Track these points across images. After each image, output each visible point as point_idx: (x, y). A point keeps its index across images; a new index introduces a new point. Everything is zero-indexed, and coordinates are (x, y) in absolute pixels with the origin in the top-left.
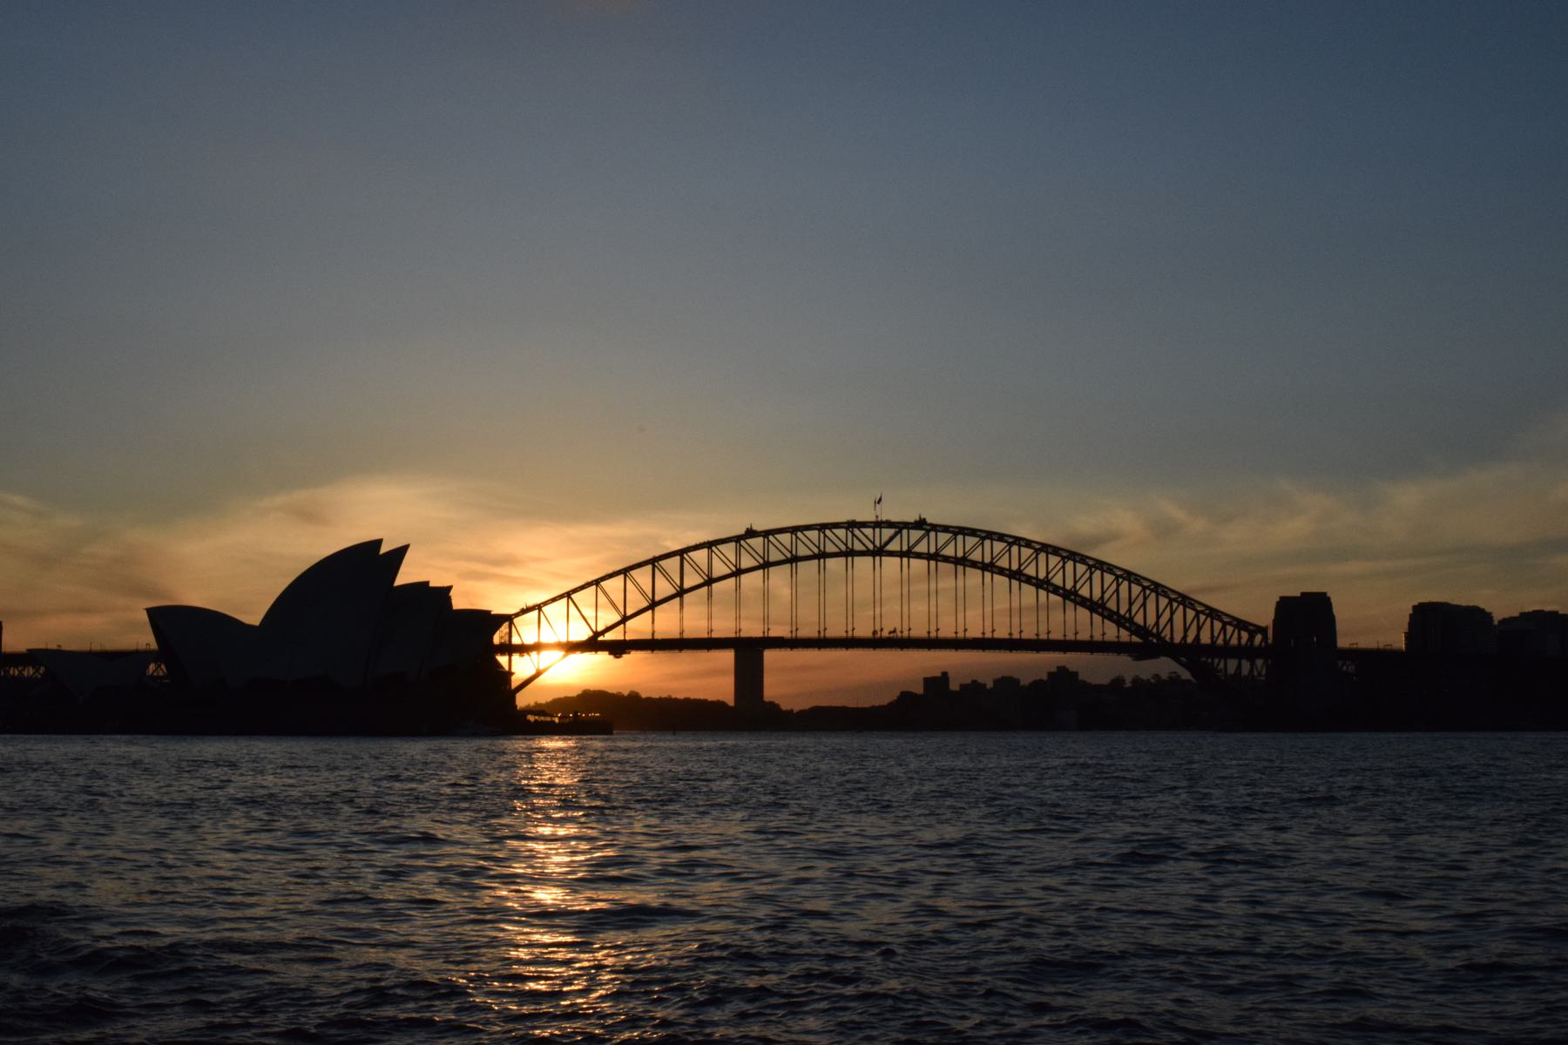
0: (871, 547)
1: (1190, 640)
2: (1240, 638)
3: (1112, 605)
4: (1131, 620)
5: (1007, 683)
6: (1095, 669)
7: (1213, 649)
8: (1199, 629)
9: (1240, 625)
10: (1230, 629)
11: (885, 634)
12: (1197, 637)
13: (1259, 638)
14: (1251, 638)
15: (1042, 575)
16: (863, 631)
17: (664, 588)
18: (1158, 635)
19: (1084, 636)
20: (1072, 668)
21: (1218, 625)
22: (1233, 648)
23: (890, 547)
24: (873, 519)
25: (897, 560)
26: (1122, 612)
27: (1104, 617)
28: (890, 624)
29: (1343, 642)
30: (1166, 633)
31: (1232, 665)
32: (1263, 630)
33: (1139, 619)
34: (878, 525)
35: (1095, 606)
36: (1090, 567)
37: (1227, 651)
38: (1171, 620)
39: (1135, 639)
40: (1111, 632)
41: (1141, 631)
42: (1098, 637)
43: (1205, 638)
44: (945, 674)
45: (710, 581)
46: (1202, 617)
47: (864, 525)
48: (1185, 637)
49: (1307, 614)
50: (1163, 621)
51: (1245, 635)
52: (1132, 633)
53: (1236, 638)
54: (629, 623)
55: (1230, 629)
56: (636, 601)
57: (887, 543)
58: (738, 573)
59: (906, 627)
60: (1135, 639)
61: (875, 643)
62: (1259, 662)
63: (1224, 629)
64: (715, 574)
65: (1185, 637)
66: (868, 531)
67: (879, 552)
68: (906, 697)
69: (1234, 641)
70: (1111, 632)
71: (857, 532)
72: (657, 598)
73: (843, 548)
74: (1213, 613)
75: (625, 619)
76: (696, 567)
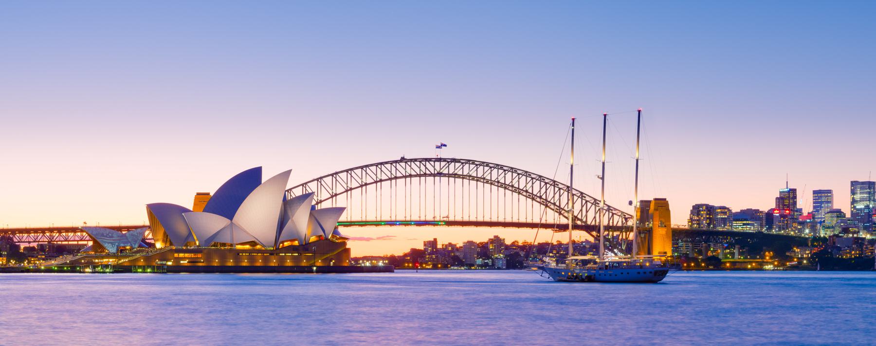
5: (470, 243)
6: (510, 236)
10: (616, 218)
20: (501, 237)
29: (672, 226)
34: (440, 160)
35: (546, 203)
36: (546, 183)
41: (575, 218)
42: (550, 221)
44: (435, 240)
53: (618, 221)
61: (419, 223)
69: (620, 224)
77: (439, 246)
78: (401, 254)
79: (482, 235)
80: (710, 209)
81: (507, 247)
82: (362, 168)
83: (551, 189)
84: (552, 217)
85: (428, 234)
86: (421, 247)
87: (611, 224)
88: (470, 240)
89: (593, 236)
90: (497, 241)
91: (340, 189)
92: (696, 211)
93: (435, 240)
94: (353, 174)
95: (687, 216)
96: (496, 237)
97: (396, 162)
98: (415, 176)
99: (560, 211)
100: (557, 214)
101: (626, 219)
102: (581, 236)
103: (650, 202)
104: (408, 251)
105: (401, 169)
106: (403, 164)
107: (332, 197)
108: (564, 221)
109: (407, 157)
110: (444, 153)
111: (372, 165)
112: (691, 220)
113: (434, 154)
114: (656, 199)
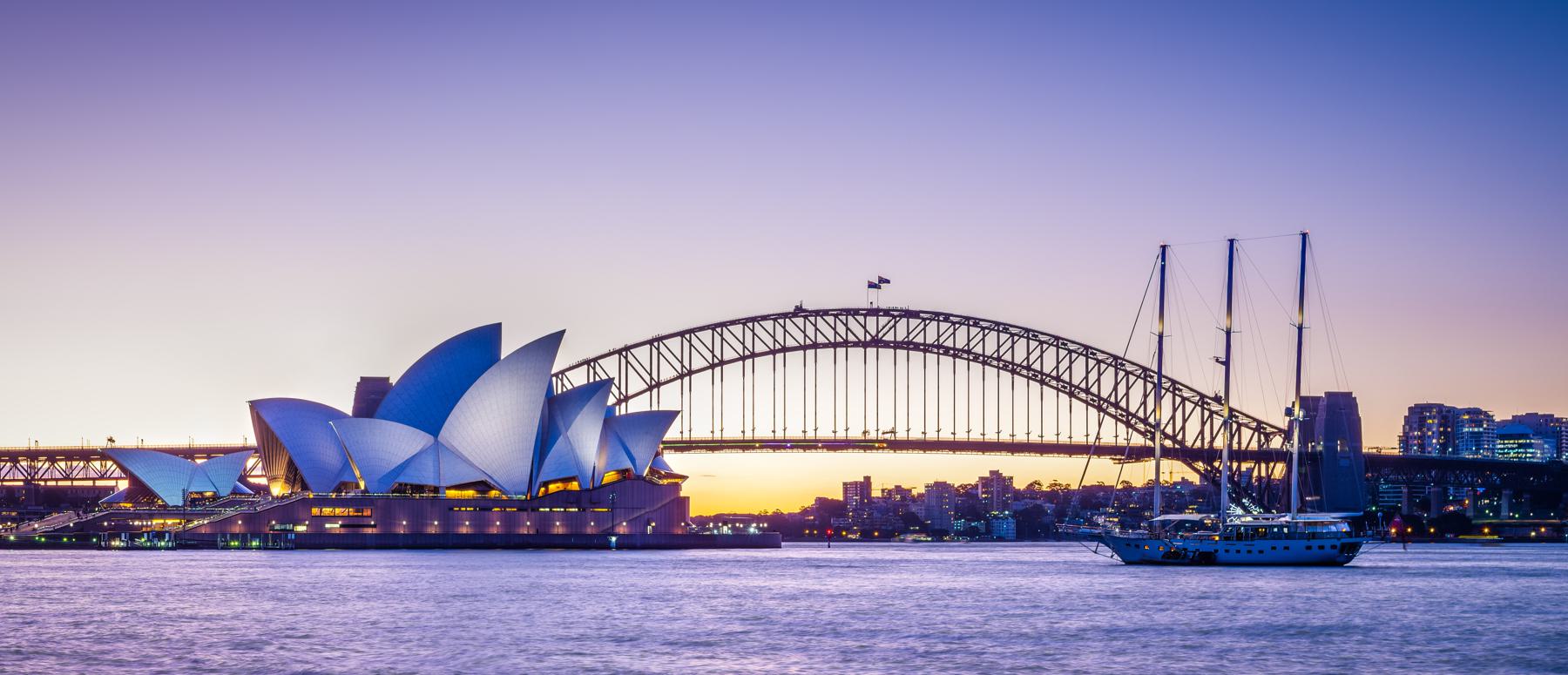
5: (940, 489)
6: (1023, 471)
9: (1260, 427)
14: (1267, 440)
22: (1252, 452)
29: (1365, 450)
30: (1180, 437)
34: (874, 312)
36: (1099, 362)
42: (1107, 439)
44: (867, 479)
47: (854, 312)
49: (1332, 416)
53: (1248, 439)
61: (834, 445)
68: (823, 505)
69: (1254, 446)
78: (785, 512)
79: (965, 470)
80: (1448, 416)
81: (1018, 495)
82: (713, 327)
83: (1051, 353)
84: (1112, 432)
85: (854, 466)
88: (941, 480)
90: (996, 482)
91: (667, 373)
92: (1416, 418)
93: (867, 479)
94: (695, 341)
95: (1398, 429)
96: (995, 474)
97: (785, 316)
98: (825, 346)
99: (1127, 419)
100: (1121, 427)
101: (1267, 436)
102: (1175, 472)
103: (1318, 399)
104: (810, 502)
105: (795, 332)
106: (799, 321)
107: (650, 388)
108: (1138, 440)
109: (807, 306)
110: (883, 299)
111: (733, 323)
112: (1405, 441)
113: (863, 299)
114: (1328, 394)
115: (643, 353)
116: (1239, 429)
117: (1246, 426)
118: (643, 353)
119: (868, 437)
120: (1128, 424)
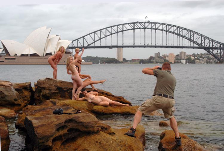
0: (144, 27)
1: (208, 46)
2: (218, 45)
3: (192, 39)
4: (196, 42)
5: (171, 54)
7: (212, 48)
8: (210, 44)
9: (218, 43)
10: (216, 44)
11: (147, 45)
12: (209, 45)
13: (222, 45)
14: (220, 45)
15: (178, 33)
16: (142, 44)
17: (103, 36)
18: (201, 45)
19: (186, 45)
21: (214, 43)
23: (148, 27)
24: (144, 21)
25: (149, 30)
26: (194, 40)
27: (191, 41)
28: (148, 43)
30: (203, 45)
31: (216, 50)
32: (222, 44)
33: (198, 42)
37: (215, 48)
38: (204, 42)
39: (197, 46)
40: (192, 44)
41: (198, 44)
42: (189, 46)
43: (211, 46)
44: (159, 53)
45: (111, 34)
46: (211, 41)
47: (142, 23)
48: (207, 45)
50: (203, 41)
51: (219, 45)
52: (196, 44)
53: (217, 45)
54: (95, 43)
55: (216, 44)
56: (97, 38)
57: (147, 26)
58: (117, 32)
59: (151, 44)
60: (197, 46)
62: (222, 50)
63: (215, 43)
64: (113, 33)
65: (207, 45)
66: (143, 24)
67: (145, 28)
68: (152, 58)
69: (217, 46)
70: (192, 44)
71: (141, 24)
72: (101, 38)
73: (138, 27)
74: (213, 40)
75: (95, 42)
76: (109, 32)
77: (161, 55)
85: (157, 50)
86: (154, 56)
87: (214, 46)
89: (206, 51)
93: (159, 53)
99: (194, 42)
100: (192, 43)
108: (195, 45)
115: (104, 31)
116: (215, 43)
117: (216, 42)
118: (104, 31)
119: (145, 45)
120: (194, 43)
